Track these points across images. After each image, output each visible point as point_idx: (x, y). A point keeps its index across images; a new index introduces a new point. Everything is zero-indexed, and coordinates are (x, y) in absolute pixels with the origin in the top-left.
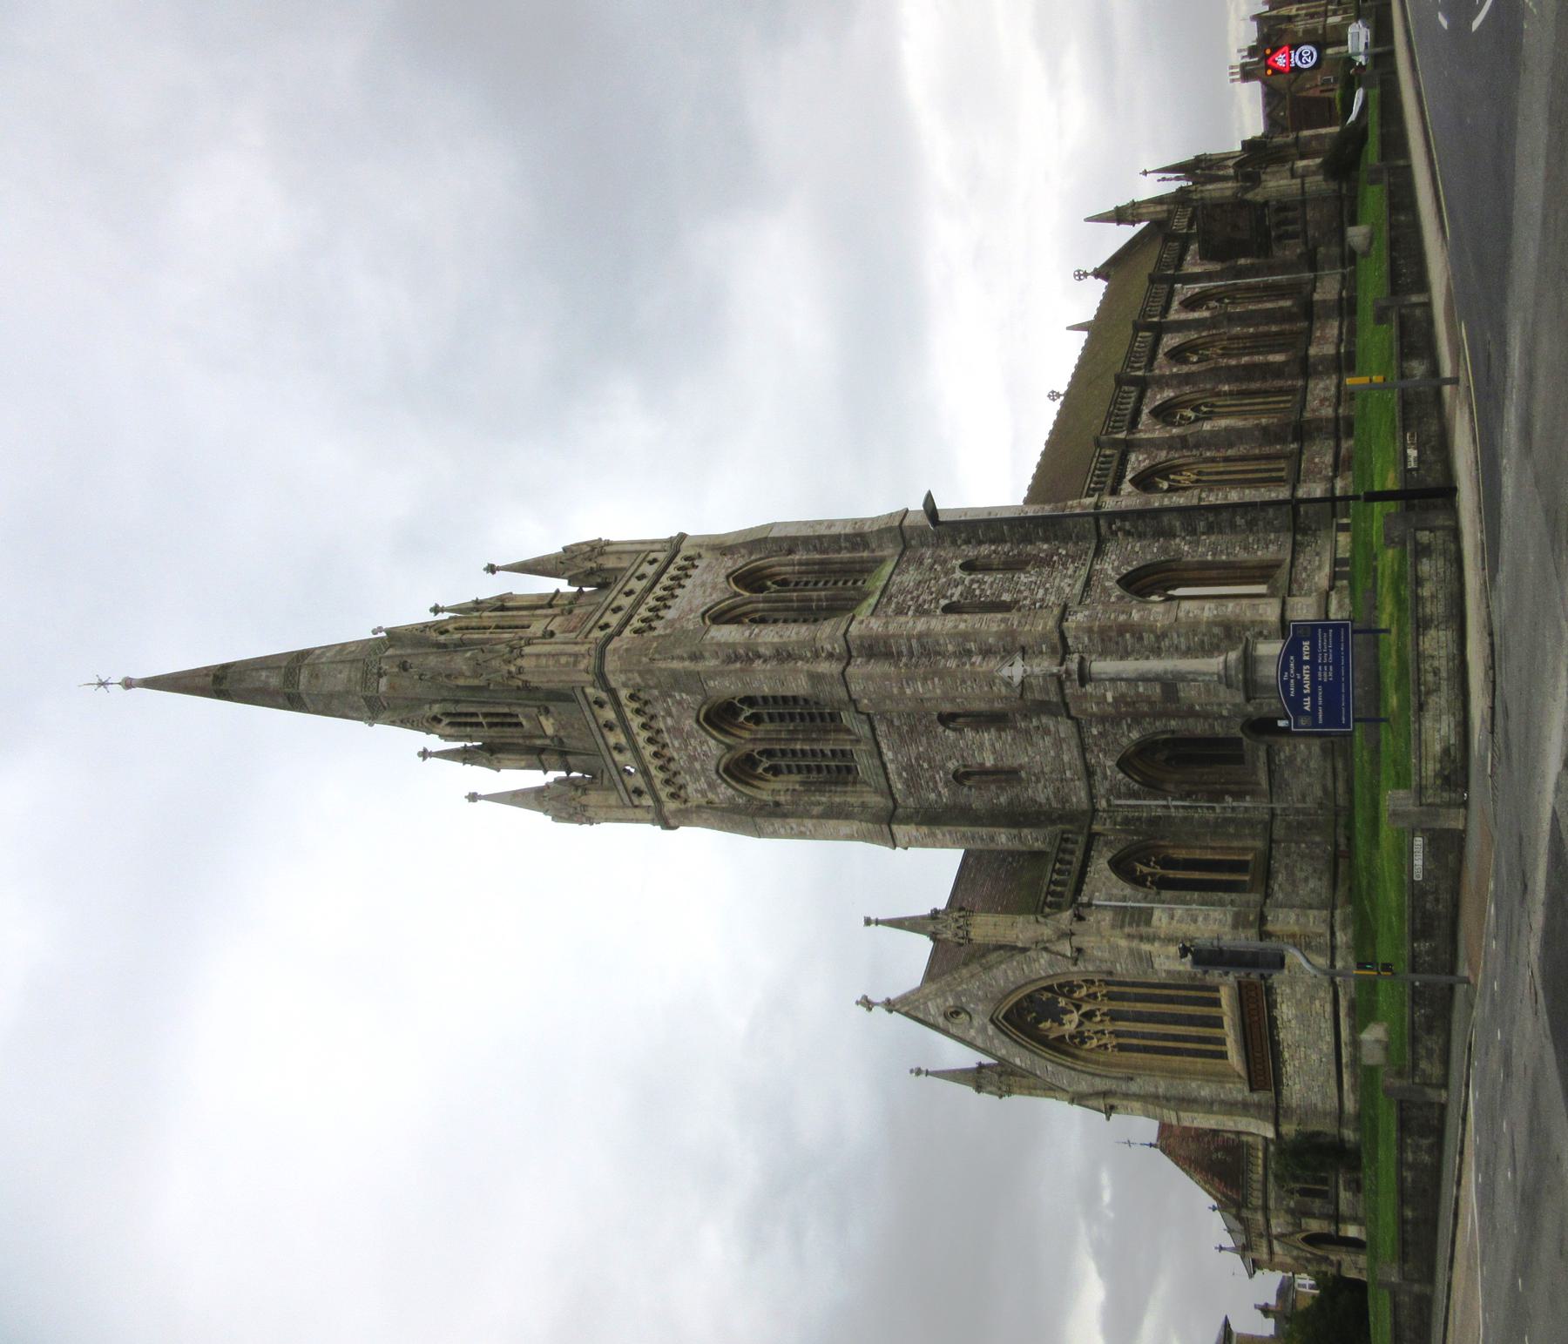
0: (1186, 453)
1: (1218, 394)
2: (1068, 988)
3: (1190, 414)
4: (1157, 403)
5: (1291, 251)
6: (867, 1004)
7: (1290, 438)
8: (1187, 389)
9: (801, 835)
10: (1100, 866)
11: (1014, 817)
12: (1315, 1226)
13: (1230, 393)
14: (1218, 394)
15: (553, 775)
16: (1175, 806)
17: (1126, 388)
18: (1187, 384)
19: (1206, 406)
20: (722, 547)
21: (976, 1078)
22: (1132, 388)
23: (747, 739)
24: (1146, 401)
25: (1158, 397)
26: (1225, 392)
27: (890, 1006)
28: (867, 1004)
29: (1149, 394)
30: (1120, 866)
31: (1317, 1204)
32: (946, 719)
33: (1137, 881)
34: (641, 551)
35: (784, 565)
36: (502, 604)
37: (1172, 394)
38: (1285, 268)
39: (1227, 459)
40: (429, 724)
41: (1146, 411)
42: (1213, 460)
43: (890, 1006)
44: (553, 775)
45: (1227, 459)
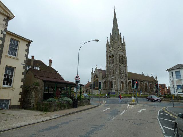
2: (98, 78)
5: (150, 91)
6: (96, 66)
9: (106, 61)
10: (105, 80)
11: (108, 74)
12: (85, 92)
15: (109, 43)
16: (109, 84)
20: (125, 55)
21: (92, 72)
23: (112, 57)
27: (96, 67)
28: (96, 66)
30: (105, 81)
31: (86, 92)
32: (113, 70)
33: (104, 82)
34: (125, 48)
35: (124, 58)
36: (121, 38)
38: (149, 90)
40: (112, 35)
43: (96, 67)
44: (109, 43)
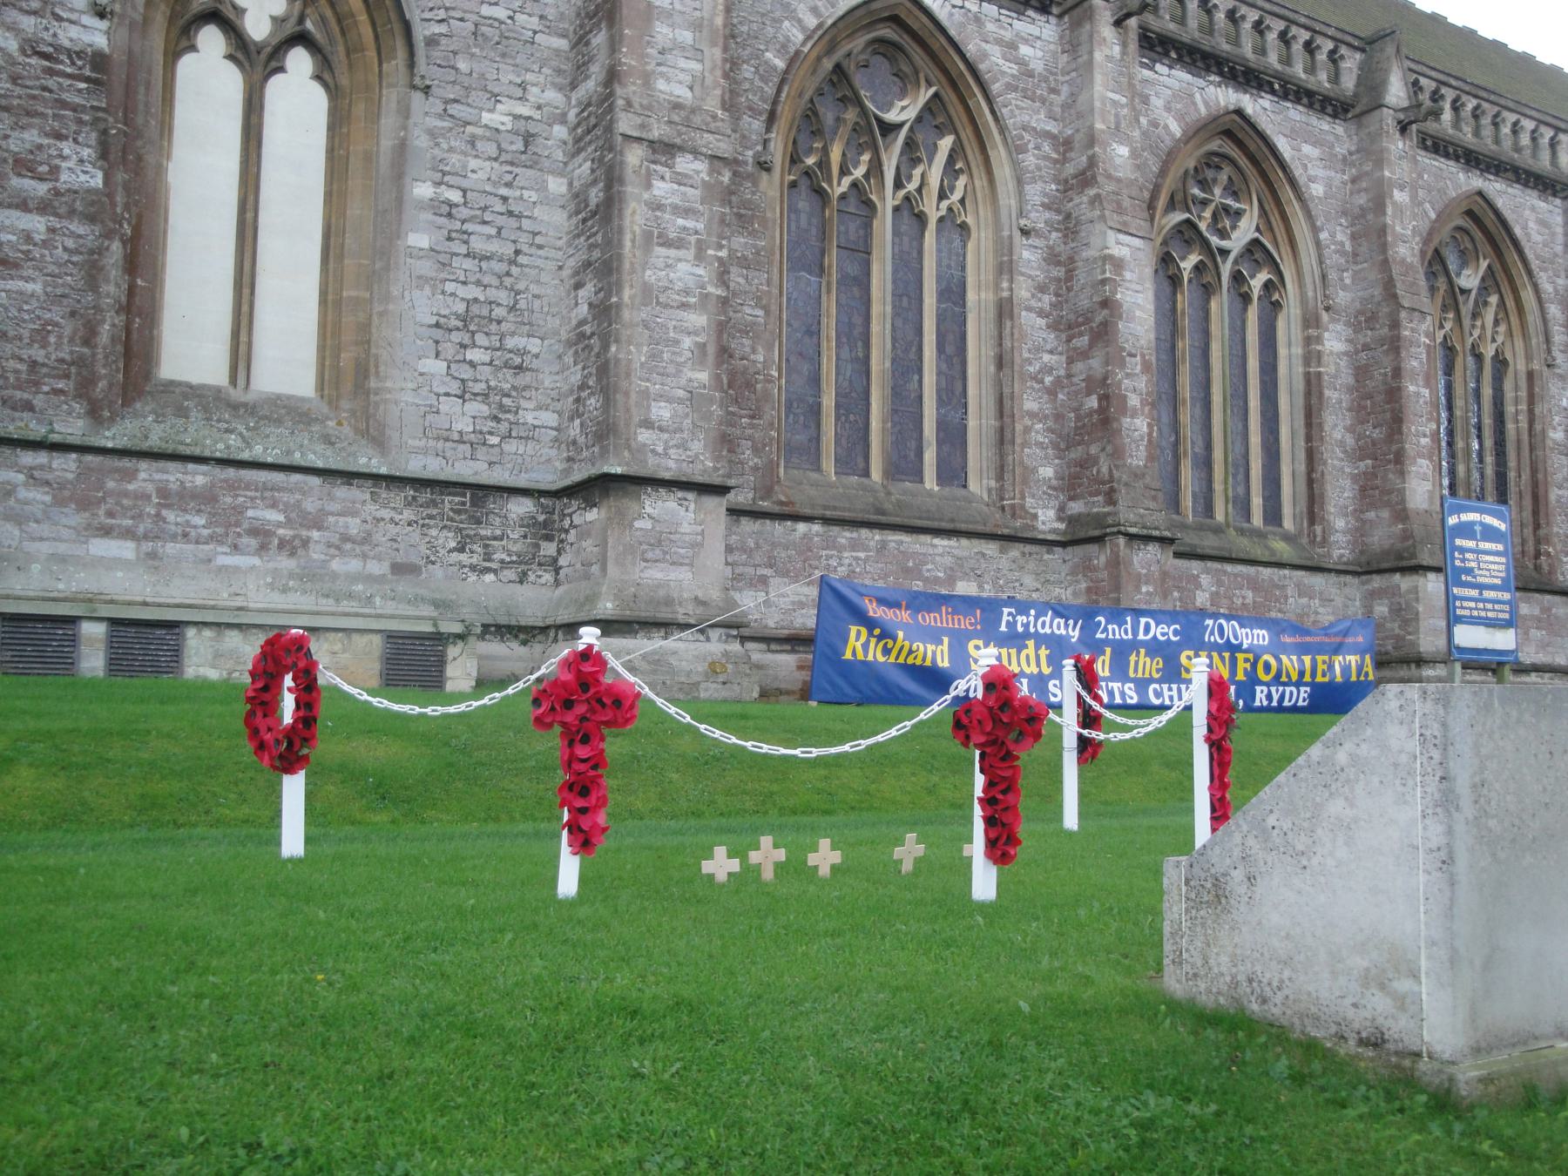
0: (1036, 193)
1: (1311, 321)
3: (1245, 231)
4: (1282, 145)
7: (1076, 507)
8: (1337, 235)
13: (1311, 356)
14: (1311, 321)
17: (1351, 63)
18: (1353, 237)
19: (1268, 286)
22: (1349, 83)
24: (1295, 113)
25: (1307, 149)
26: (1319, 340)
29: (1324, 125)
37: (1317, 190)
39: (1004, 311)
41: (1257, 106)
42: (1006, 267)
45: (1004, 311)
